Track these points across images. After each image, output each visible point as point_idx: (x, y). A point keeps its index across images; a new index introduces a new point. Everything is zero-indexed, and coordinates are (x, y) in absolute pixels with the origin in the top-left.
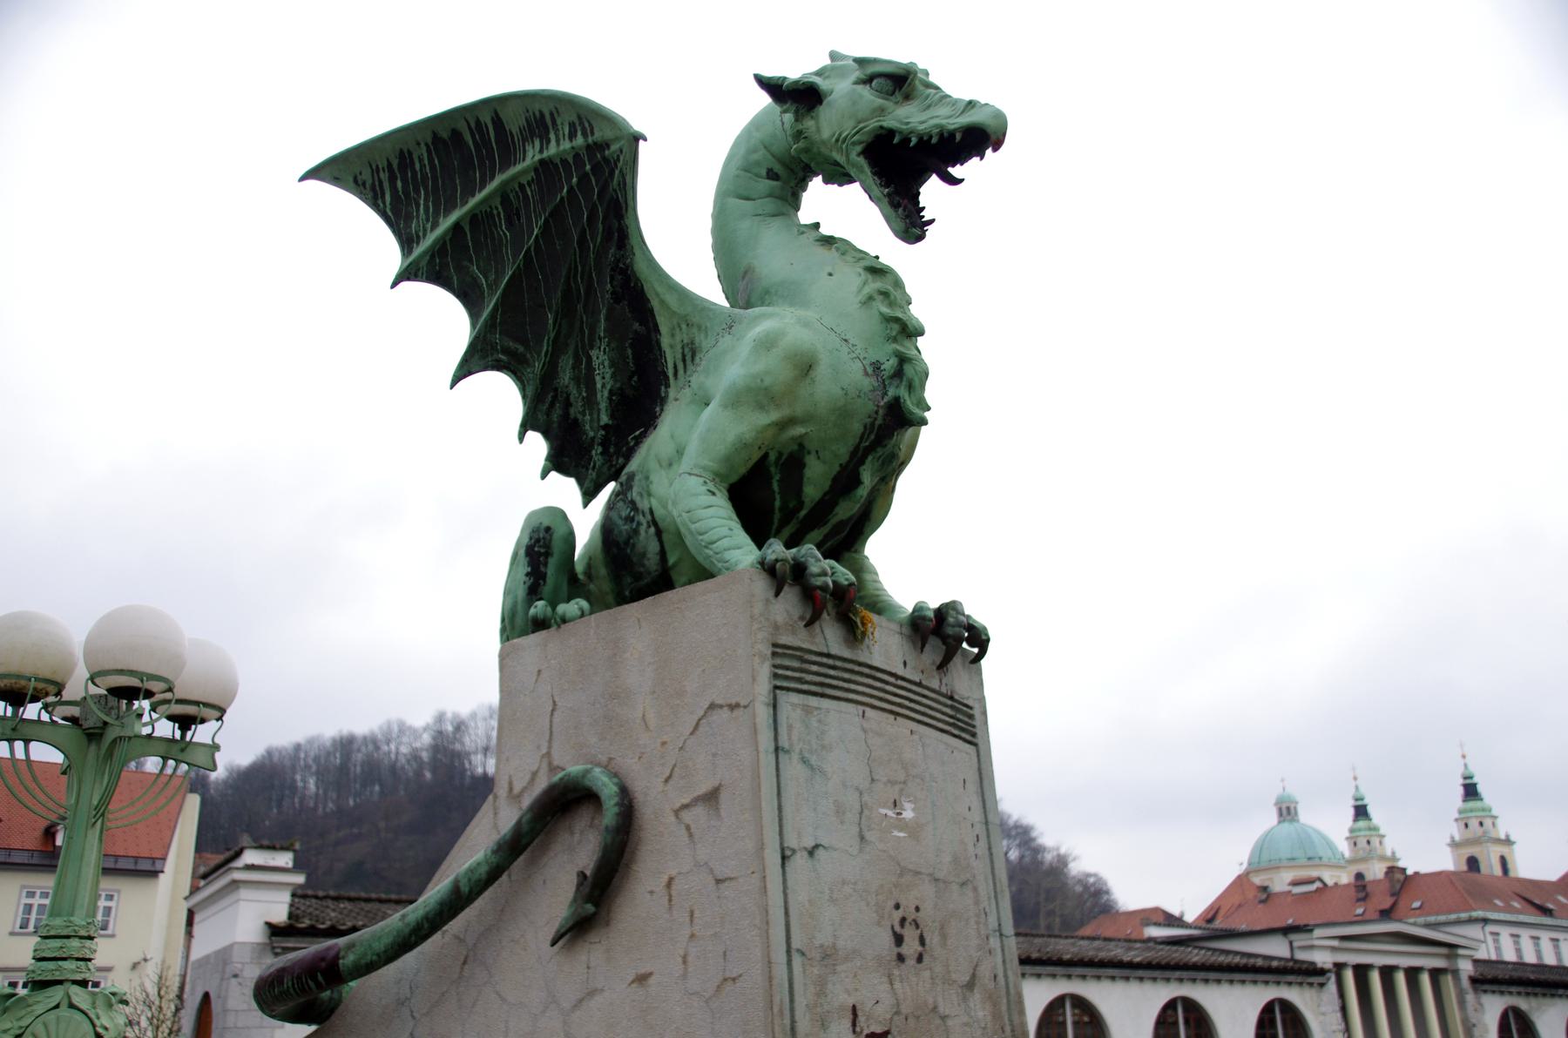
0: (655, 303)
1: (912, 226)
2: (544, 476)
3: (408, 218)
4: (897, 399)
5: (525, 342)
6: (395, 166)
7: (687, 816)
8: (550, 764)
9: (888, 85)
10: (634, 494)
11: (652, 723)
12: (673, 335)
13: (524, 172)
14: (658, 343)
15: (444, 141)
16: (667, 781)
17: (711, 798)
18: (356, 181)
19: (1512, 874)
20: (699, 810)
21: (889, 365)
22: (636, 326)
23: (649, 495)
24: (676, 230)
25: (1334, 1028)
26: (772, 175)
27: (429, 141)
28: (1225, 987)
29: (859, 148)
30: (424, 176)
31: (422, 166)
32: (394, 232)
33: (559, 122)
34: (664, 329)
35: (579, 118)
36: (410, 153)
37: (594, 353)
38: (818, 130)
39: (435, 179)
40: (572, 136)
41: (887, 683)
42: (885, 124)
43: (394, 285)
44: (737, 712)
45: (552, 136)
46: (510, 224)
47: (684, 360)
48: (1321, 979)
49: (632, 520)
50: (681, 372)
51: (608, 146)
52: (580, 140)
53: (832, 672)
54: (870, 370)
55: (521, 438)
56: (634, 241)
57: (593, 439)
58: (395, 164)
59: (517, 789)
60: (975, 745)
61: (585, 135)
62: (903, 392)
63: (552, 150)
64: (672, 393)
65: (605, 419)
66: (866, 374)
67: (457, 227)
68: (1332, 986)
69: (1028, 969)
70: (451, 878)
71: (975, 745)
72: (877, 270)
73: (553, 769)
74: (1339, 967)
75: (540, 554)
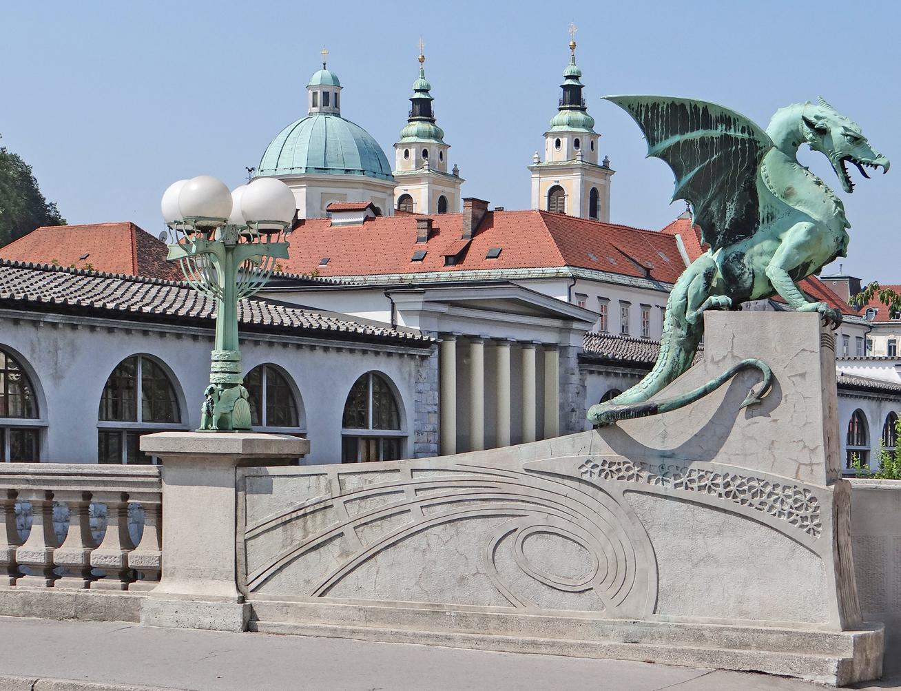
1: (850, 187)
3: (653, 130)
5: (699, 193)
6: (650, 107)
7: (793, 379)
8: (732, 355)
9: (853, 139)
10: (745, 261)
11: (779, 350)
12: (764, 208)
14: (757, 209)
15: (676, 106)
16: (785, 368)
17: (803, 375)
18: (629, 106)
19: (600, 214)
20: (798, 377)
21: (840, 239)
22: (750, 201)
23: (752, 264)
25: (430, 409)
27: (669, 104)
28: (319, 353)
30: (662, 115)
31: (663, 110)
32: (644, 132)
33: (737, 123)
35: (748, 127)
36: (659, 105)
37: (728, 204)
38: (823, 144)
39: (667, 119)
40: (743, 131)
44: (813, 353)
45: (732, 126)
46: (701, 146)
47: (768, 217)
48: (424, 352)
49: (742, 270)
50: (766, 222)
51: (759, 142)
52: (746, 136)
57: (719, 232)
58: (650, 106)
59: (716, 359)
61: (749, 133)
63: (732, 133)
64: (761, 227)
65: (727, 227)
67: (679, 142)
68: (434, 361)
69: (247, 335)
70: (703, 387)
72: (839, 203)
73: (734, 357)
74: (444, 335)
75: (710, 277)
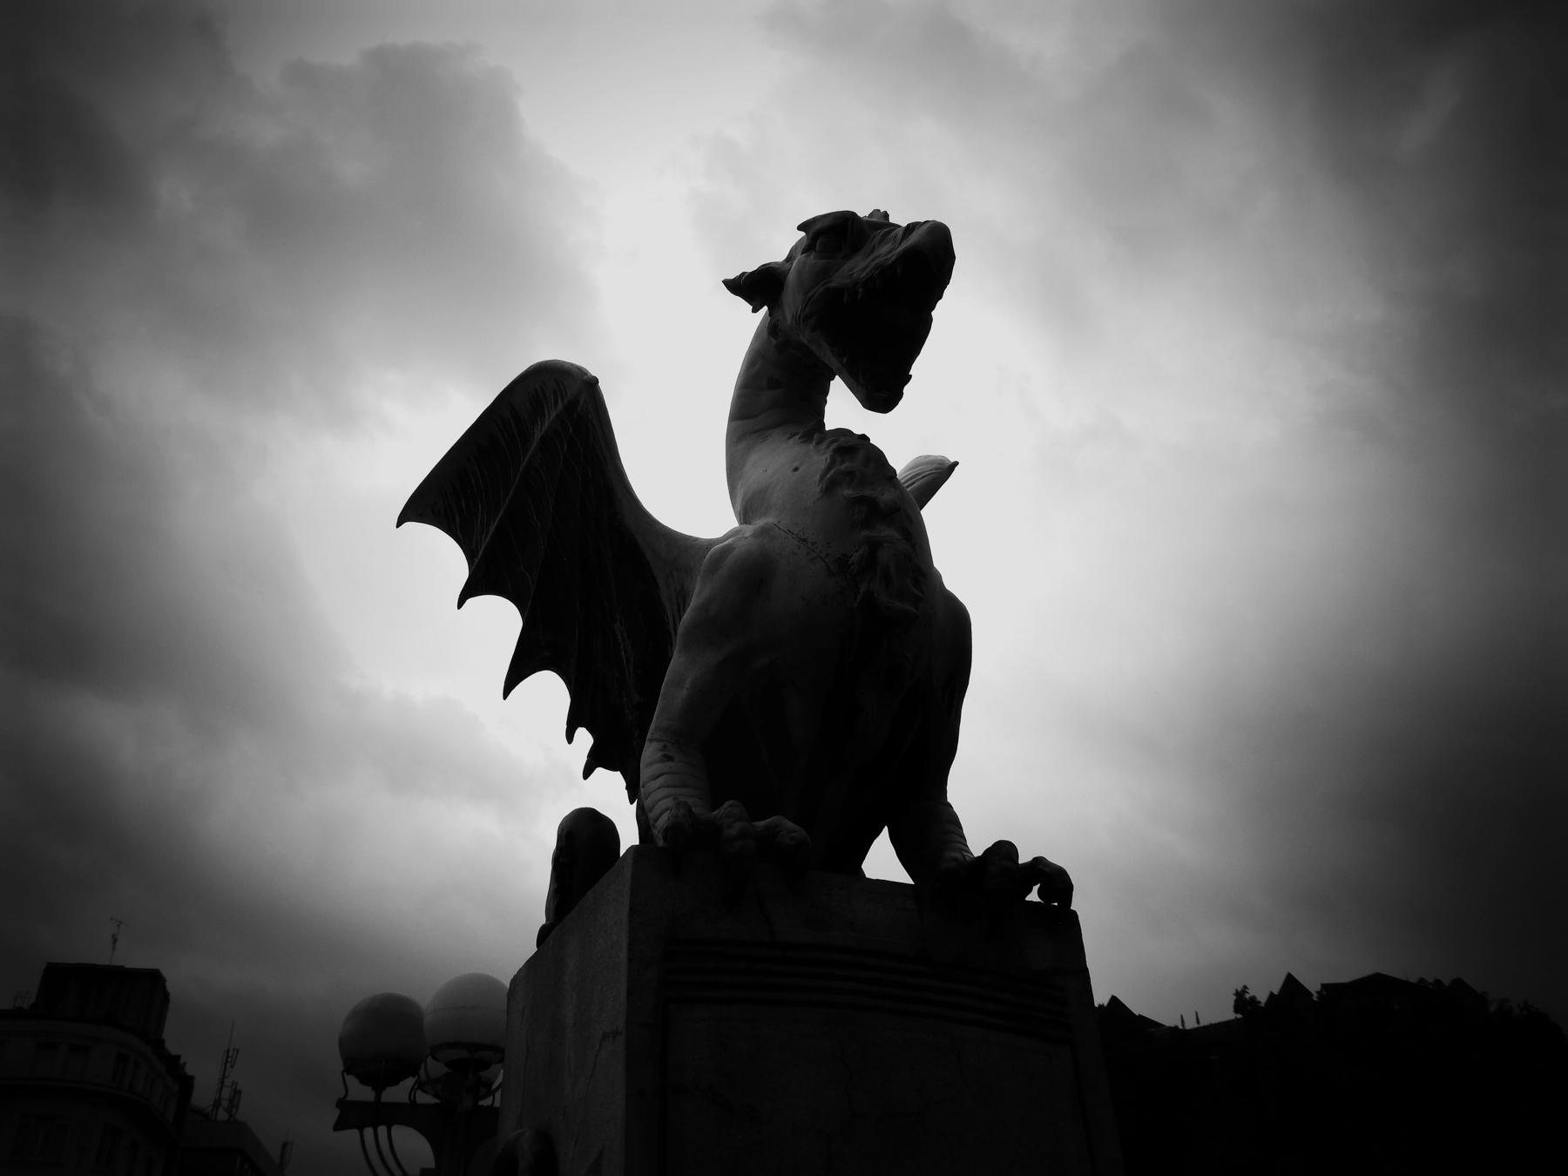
2: (587, 773)
34: (661, 582)
40: (556, 403)
55: (570, 737)
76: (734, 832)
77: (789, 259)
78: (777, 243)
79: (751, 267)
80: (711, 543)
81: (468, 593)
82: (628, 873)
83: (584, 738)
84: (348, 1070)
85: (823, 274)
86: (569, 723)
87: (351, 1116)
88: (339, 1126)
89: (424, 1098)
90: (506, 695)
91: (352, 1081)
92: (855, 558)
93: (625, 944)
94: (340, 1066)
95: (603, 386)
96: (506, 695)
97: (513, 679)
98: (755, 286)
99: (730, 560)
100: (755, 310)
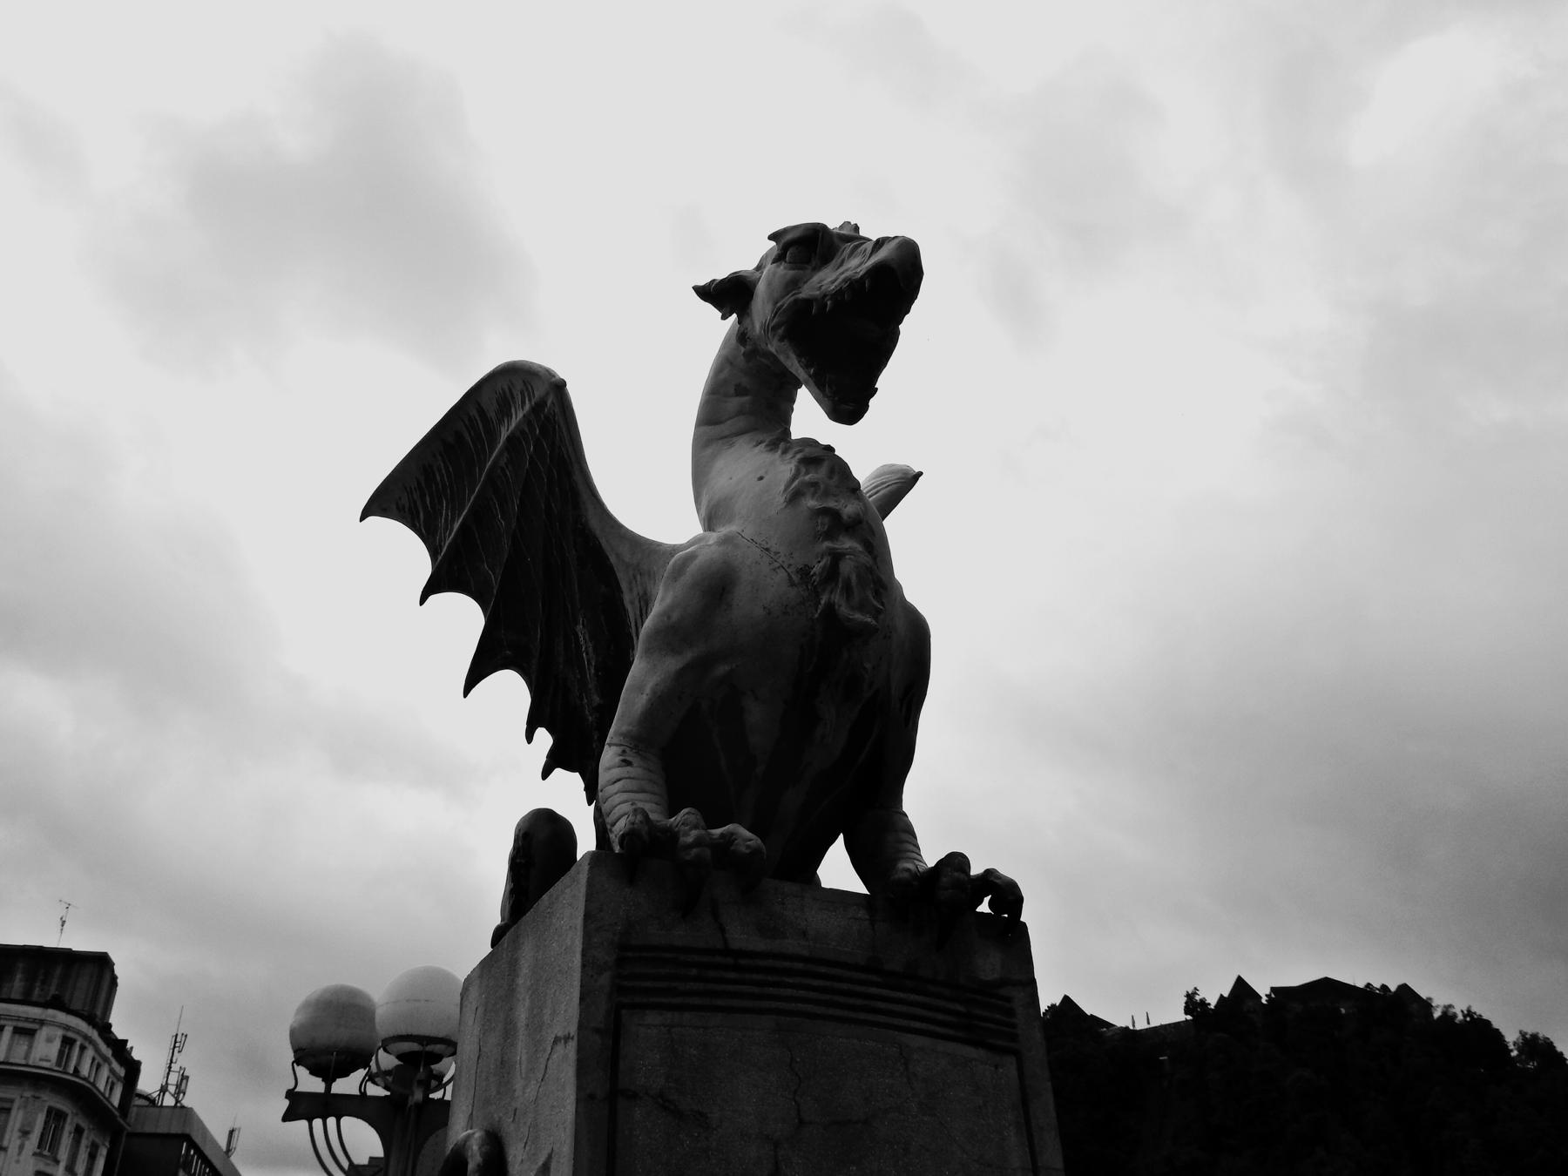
0: (613, 559)
2: (546, 773)
4: (830, 607)
13: (500, 454)
24: (647, 477)
26: (740, 391)
29: (780, 331)
34: (624, 586)
40: (523, 403)
41: (840, 979)
42: (801, 296)
43: (422, 601)
53: (732, 975)
54: (796, 578)
55: (529, 737)
56: (585, 496)
60: (1016, 1053)
62: (837, 598)
66: (792, 584)
71: (1016, 1053)
76: (690, 839)
77: (759, 268)
78: (745, 251)
79: (722, 274)
80: (674, 549)
81: (430, 589)
82: (583, 878)
83: (544, 739)
84: (298, 1061)
85: (793, 285)
86: (529, 723)
87: (300, 1107)
88: (288, 1117)
89: (374, 1090)
90: (465, 695)
91: (302, 1072)
92: (817, 569)
93: (579, 949)
94: (290, 1056)
95: (572, 390)
96: (465, 695)
97: (475, 676)
98: (727, 294)
99: (693, 568)
100: (724, 317)
